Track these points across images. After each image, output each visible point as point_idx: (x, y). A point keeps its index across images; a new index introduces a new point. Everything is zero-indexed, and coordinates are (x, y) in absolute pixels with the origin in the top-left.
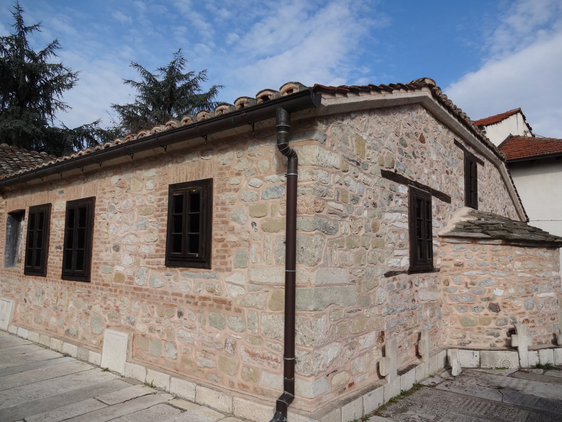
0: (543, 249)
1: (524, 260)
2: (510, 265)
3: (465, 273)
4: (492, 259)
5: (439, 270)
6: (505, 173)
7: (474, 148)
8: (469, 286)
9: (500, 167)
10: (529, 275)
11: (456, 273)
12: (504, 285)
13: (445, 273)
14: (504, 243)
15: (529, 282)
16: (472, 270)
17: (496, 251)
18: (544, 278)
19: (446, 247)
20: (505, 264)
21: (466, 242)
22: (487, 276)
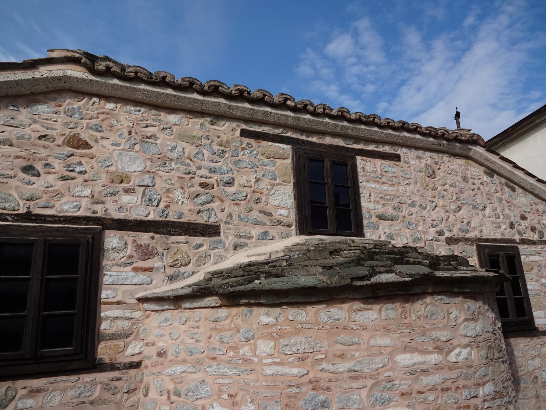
0: (346, 306)
1: (281, 336)
2: (247, 348)
3: (168, 371)
4: (210, 338)
5: (138, 365)
6: (494, 163)
7: (334, 135)
8: (173, 398)
9: (471, 154)
10: (295, 371)
11: (157, 369)
12: (231, 396)
13: (146, 371)
14: (226, 303)
15: (298, 386)
16: (177, 363)
17: (216, 321)
18: (354, 375)
19: (150, 318)
20: (235, 349)
21: (166, 307)
22: (199, 376)
